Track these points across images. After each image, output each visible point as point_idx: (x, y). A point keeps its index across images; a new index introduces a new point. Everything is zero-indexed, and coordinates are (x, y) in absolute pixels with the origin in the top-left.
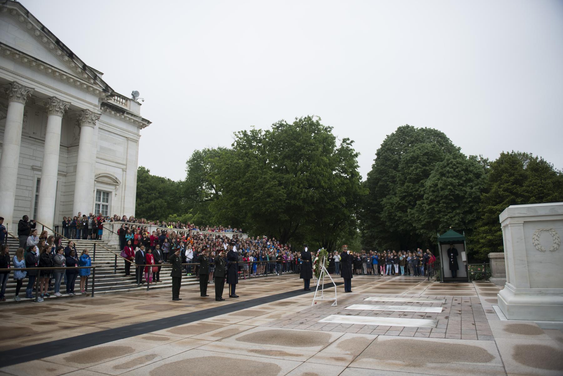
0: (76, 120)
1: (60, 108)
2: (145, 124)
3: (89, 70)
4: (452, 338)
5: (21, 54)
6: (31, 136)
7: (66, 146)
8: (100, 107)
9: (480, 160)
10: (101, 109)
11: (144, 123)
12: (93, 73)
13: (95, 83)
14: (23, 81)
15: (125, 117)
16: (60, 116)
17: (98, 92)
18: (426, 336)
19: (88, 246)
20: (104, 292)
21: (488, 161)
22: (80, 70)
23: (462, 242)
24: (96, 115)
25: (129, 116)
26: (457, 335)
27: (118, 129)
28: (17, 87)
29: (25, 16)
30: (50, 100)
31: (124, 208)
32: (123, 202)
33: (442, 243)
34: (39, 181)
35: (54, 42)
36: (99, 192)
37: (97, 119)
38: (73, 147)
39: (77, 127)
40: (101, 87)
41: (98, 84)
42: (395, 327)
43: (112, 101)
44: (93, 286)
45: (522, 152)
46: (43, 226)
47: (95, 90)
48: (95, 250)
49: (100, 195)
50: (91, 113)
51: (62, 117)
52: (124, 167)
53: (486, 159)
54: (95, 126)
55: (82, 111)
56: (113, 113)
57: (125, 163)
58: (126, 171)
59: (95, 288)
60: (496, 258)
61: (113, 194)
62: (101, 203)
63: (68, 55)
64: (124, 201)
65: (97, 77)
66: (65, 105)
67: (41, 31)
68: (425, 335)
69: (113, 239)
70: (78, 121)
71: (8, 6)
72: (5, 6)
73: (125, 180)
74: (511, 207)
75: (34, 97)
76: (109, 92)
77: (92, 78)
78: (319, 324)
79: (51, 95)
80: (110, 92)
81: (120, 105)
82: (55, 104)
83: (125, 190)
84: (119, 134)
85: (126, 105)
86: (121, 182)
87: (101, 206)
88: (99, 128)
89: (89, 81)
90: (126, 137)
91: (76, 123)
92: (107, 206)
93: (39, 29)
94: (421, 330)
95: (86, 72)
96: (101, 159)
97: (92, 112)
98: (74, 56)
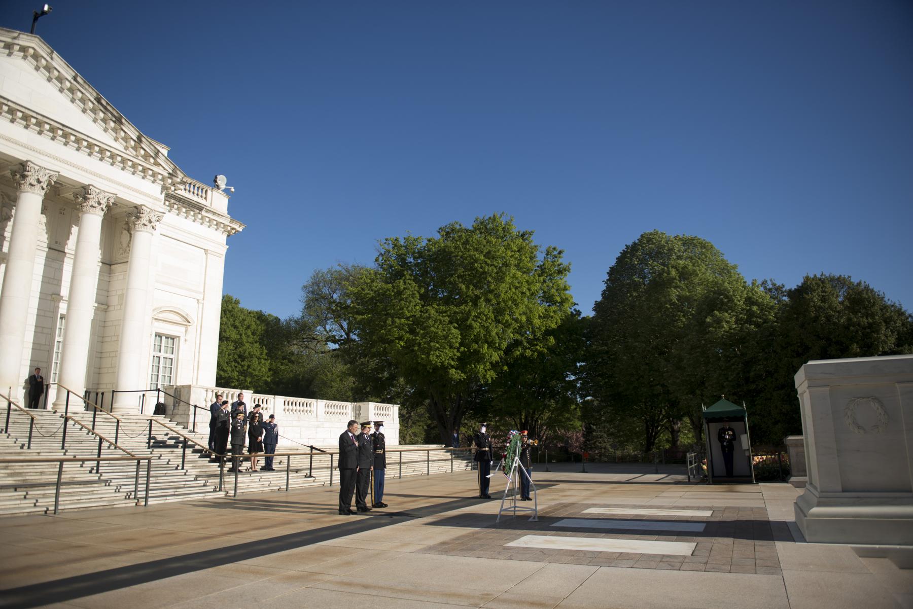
0: (125, 222)
1: (99, 204)
2: (235, 229)
4: (715, 570)
5: (39, 117)
7: (107, 262)
8: (163, 201)
9: (771, 286)
10: (164, 204)
11: (234, 226)
13: (157, 164)
14: (42, 160)
16: (100, 216)
17: (160, 177)
18: (675, 568)
19: (140, 423)
20: (165, 498)
21: (784, 289)
22: (133, 143)
23: (742, 419)
24: (157, 213)
26: (723, 567)
28: (32, 170)
29: (48, 59)
30: (83, 190)
31: (198, 362)
35: (92, 99)
37: (158, 221)
38: (119, 265)
39: (125, 232)
40: (164, 169)
41: (160, 165)
42: (628, 554)
43: (182, 192)
44: (147, 490)
45: (837, 275)
47: (154, 175)
50: (148, 210)
52: (200, 297)
53: (781, 284)
55: (135, 207)
56: (184, 210)
58: (203, 304)
62: (162, 354)
63: (114, 119)
64: (199, 352)
65: (160, 154)
66: (108, 199)
67: (72, 81)
68: (673, 566)
70: (127, 223)
71: (21, 43)
72: (16, 41)
74: (810, 363)
75: (58, 186)
76: (177, 177)
77: (151, 156)
78: (509, 549)
79: (86, 182)
80: (180, 177)
81: (195, 198)
82: (91, 196)
85: (206, 198)
86: (195, 320)
88: (161, 234)
89: (146, 160)
90: (205, 249)
91: (124, 226)
92: (172, 359)
93: (70, 78)
94: (668, 559)
95: (143, 146)
98: (123, 121)
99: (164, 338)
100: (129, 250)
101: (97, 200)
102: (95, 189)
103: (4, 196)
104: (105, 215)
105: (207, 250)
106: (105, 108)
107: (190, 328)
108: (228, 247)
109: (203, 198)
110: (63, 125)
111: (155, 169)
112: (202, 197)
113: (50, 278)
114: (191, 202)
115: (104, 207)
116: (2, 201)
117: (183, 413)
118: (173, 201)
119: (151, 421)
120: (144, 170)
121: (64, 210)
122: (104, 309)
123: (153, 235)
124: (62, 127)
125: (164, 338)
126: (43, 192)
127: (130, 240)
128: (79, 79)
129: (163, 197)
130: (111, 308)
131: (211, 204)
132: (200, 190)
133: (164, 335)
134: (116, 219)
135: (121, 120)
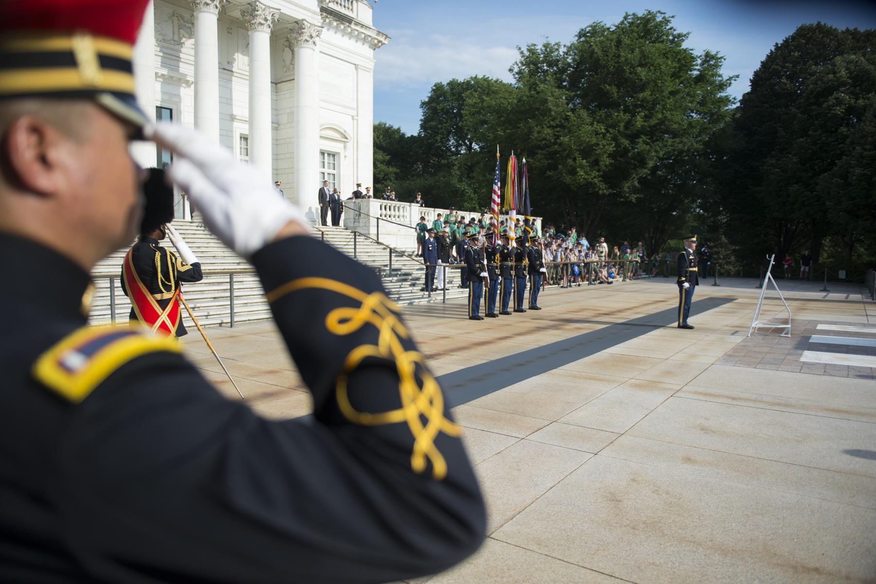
0: (286, 39)
1: (266, 20)
6: (226, 68)
11: (380, 38)
15: (351, 30)
16: (268, 33)
19: (331, 235)
24: (316, 28)
25: (358, 28)
30: (250, 7)
32: (355, 169)
36: (323, 153)
37: (317, 36)
39: (287, 49)
49: (324, 159)
50: (309, 25)
51: (270, 34)
52: (354, 113)
54: (316, 47)
55: (296, 22)
56: (335, 24)
58: (357, 120)
62: (326, 170)
64: (357, 168)
66: (273, 14)
69: (361, 224)
70: (288, 40)
73: (357, 134)
83: (357, 150)
85: (352, 10)
86: (352, 135)
88: (321, 52)
90: (355, 64)
91: (286, 43)
92: (334, 175)
97: (311, 24)
99: (326, 155)
100: (293, 68)
101: (264, 17)
102: (261, 5)
103: (179, 18)
104: (272, 32)
105: (358, 65)
107: (348, 144)
109: (350, 10)
112: (348, 8)
113: (227, 99)
114: (341, 15)
115: (269, 23)
116: (178, 23)
117: (364, 225)
118: (325, 14)
121: (231, 29)
122: (275, 128)
123: (314, 50)
126: (217, 11)
127: (293, 57)
129: (318, 10)
130: (281, 127)
131: (357, 15)
133: (326, 151)
134: (276, 36)
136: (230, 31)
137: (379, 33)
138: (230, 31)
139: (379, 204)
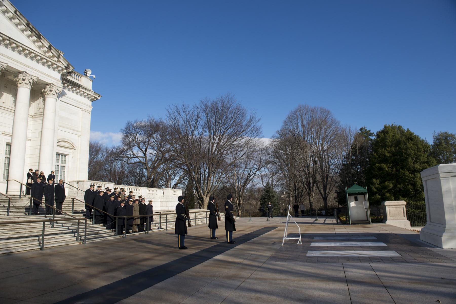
0: (40, 93)
3: (54, 49)
12: (57, 52)
13: (59, 61)
20: (92, 240)
24: (59, 88)
25: (84, 90)
27: (74, 101)
33: (349, 195)
34: (9, 145)
35: (25, 24)
40: (63, 64)
43: (69, 78)
44: (85, 235)
46: (21, 184)
47: (58, 67)
48: (73, 204)
52: (80, 134)
57: (80, 131)
59: (87, 237)
60: (389, 205)
61: (70, 156)
62: (60, 164)
63: (36, 36)
65: (61, 56)
67: (14, 13)
76: (70, 69)
77: (56, 57)
80: (71, 69)
84: (75, 105)
87: (60, 166)
88: (60, 101)
93: (12, 12)
95: (52, 51)
96: (60, 126)
98: (41, 37)
99: (60, 155)
106: (32, 29)
108: (92, 107)
110: (10, 38)
111: (58, 64)
118: (65, 82)
119: (73, 199)
120: (53, 64)
124: (8, 39)
125: (60, 155)
128: (18, 13)
132: (78, 76)
133: (61, 154)
135: (40, 37)
136: (6, 86)
137: (95, 93)
138: (6, 86)
139: (91, 183)
